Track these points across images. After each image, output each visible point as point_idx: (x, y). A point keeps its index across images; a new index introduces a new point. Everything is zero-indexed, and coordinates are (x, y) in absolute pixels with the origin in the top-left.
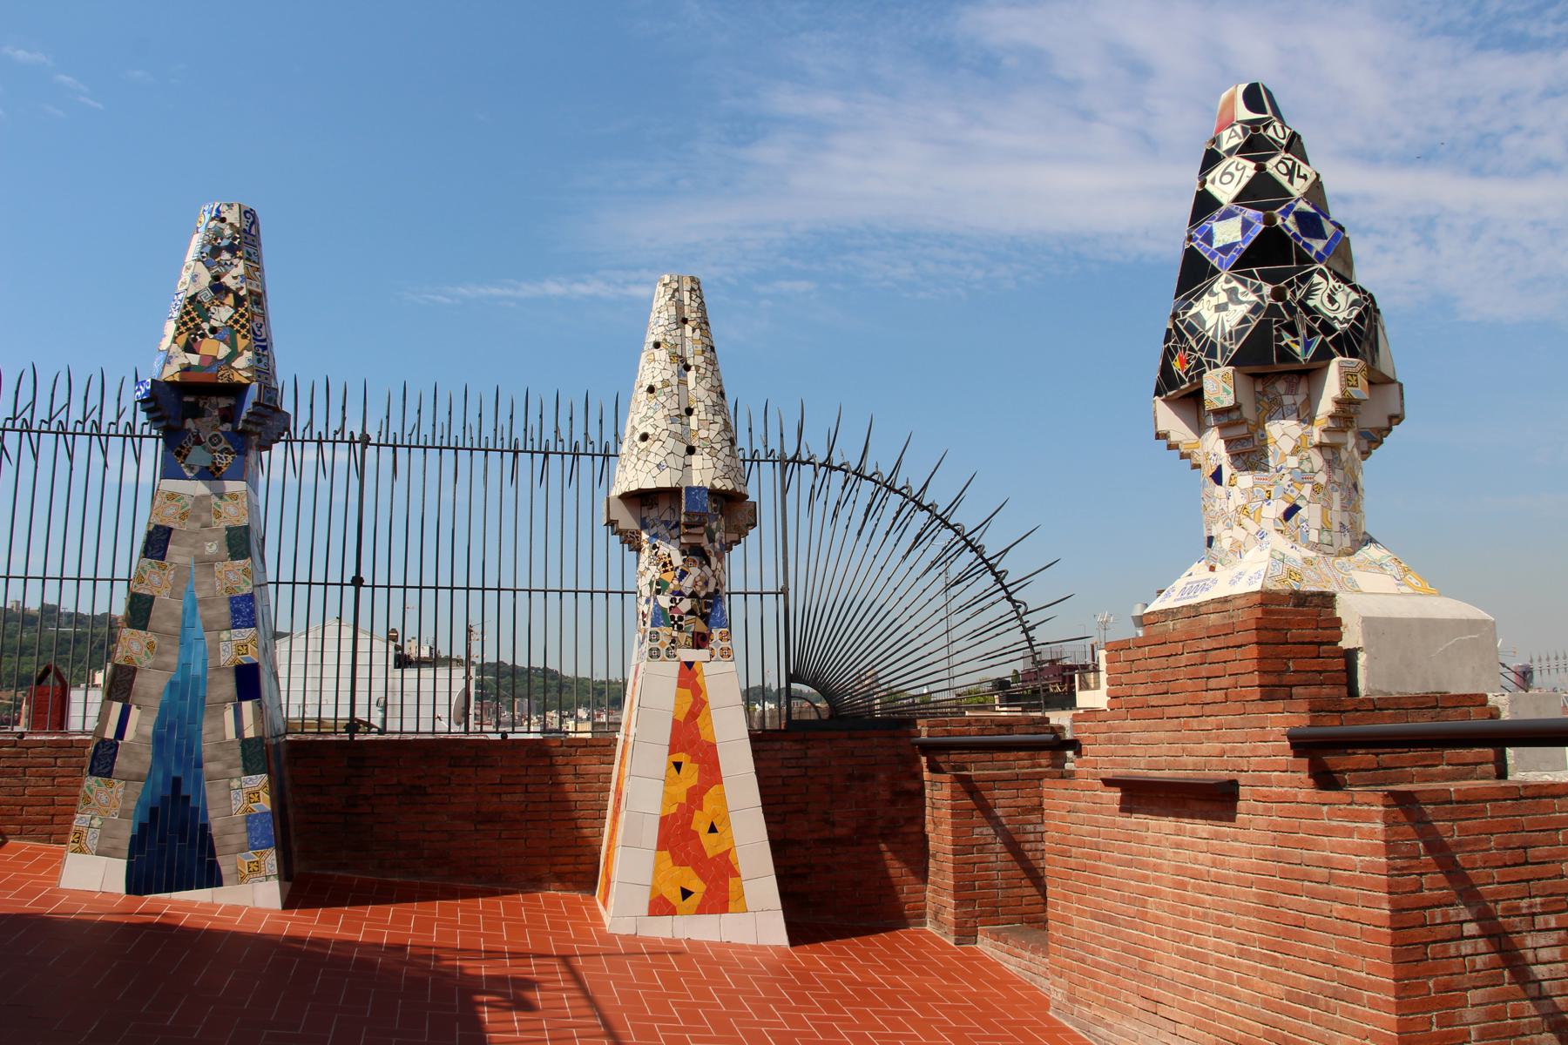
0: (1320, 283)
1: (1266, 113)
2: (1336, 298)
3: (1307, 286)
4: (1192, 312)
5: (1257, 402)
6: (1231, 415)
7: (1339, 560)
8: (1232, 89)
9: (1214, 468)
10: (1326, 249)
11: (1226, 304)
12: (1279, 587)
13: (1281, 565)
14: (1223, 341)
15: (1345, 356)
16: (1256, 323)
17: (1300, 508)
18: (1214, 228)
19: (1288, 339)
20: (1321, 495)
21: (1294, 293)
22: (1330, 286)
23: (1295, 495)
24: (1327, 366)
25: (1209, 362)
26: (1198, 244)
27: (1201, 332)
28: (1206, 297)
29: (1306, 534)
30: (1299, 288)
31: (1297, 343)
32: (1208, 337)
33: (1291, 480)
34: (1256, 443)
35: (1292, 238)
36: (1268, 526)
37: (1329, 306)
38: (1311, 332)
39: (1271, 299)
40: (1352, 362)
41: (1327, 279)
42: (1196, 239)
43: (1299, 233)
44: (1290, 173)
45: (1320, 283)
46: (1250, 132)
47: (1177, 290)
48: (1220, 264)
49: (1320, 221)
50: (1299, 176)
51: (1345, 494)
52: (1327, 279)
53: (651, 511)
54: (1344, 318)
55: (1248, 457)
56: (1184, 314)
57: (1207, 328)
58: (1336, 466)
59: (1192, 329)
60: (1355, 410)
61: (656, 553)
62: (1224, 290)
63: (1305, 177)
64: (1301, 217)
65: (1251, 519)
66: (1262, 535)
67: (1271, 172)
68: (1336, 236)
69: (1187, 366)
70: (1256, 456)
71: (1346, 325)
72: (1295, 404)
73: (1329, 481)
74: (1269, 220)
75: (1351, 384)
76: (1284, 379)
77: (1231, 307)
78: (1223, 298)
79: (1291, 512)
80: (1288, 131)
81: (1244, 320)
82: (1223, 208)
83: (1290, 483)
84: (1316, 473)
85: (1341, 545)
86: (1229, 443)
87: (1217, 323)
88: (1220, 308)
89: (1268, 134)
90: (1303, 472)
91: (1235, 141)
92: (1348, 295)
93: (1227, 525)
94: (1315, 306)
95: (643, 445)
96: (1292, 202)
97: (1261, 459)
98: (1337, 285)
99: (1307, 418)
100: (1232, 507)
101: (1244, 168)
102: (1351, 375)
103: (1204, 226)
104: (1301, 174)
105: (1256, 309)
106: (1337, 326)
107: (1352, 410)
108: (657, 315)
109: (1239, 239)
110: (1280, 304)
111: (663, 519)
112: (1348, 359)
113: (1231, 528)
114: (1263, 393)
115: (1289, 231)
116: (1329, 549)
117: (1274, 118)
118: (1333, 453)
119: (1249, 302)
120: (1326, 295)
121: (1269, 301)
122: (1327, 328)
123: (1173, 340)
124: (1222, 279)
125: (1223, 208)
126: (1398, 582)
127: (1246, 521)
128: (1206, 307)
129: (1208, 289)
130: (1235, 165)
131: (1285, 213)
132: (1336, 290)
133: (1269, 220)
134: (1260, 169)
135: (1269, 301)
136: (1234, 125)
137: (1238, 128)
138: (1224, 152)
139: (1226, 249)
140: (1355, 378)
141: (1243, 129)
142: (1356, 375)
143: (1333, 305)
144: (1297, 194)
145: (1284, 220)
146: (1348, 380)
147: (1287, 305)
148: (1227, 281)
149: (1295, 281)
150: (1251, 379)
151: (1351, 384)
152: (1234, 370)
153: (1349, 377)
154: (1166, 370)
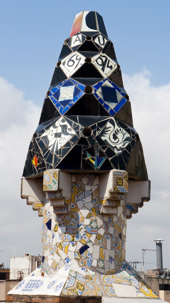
0: (110, 127)
1: (96, 29)
2: (118, 136)
4: (44, 135)
5: (72, 187)
6: (56, 195)
7: (107, 277)
8: (81, 13)
9: (48, 220)
10: (116, 108)
11: (60, 134)
12: (71, 294)
13: (74, 281)
14: (56, 154)
15: (117, 169)
16: (73, 147)
17: (89, 247)
18: (61, 90)
19: (89, 157)
20: (100, 241)
21: (95, 132)
22: (115, 129)
24: (108, 173)
25: (48, 165)
26: (52, 98)
27: (46, 147)
28: (51, 128)
29: (90, 262)
30: (98, 130)
31: (94, 160)
32: (49, 151)
33: (85, 232)
34: (69, 210)
36: (71, 256)
37: (113, 140)
38: (102, 154)
39: (83, 135)
40: (121, 173)
41: (114, 125)
42: (51, 94)
43: (103, 99)
44: (103, 65)
45: (110, 127)
46: (86, 39)
47: (40, 121)
48: (61, 111)
49: (115, 93)
50: (108, 66)
51: (113, 240)
52: (114, 125)
54: (120, 147)
55: (65, 217)
56: (40, 135)
57: (49, 146)
58: (110, 225)
59: (41, 144)
60: (121, 198)
63: (111, 67)
64: (105, 90)
65: (63, 251)
66: (68, 260)
67: (93, 63)
68: (123, 101)
69: (38, 164)
70: (69, 217)
71: (120, 151)
73: (105, 233)
74: (88, 90)
75: (119, 184)
76: (87, 176)
77: (63, 136)
78: (59, 130)
79: (84, 249)
80: (106, 41)
81: (68, 144)
82: (67, 80)
83: (84, 233)
84: (99, 229)
85: (109, 268)
86: (56, 208)
87: (55, 143)
88: (57, 135)
89: (95, 41)
90: (92, 227)
91: (78, 43)
92: (124, 135)
93: (51, 252)
94: (105, 140)
96: (102, 81)
98: (119, 129)
99: (97, 199)
100: (54, 243)
101: (80, 59)
102: (120, 179)
103: (56, 88)
104: (109, 65)
105: (74, 139)
106: (116, 151)
107: (119, 197)
109: (72, 98)
110: (87, 137)
112: (119, 170)
113: (53, 254)
114: (75, 183)
115: (98, 97)
116: (102, 271)
117: (100, 33)
118: (109, 218)
119: (71, 135)
120: (112, 134)
121: (81, 135)
122: (110, 152)
123: (33, 149)
124: (61, 119)
125: (67, 80)
126: (137, 290)
127: (61, 252)
128: (51, 133)
129: (53, 124)
130: (75, 56)
131: (97, 87)
132: (118, 131)
133: (88, 90)
134: (88, 60)
135: (81, 135)
136: (78, 34)
137: (80, 36)
138: (72, 48)
139: (65, 102)
140: (121, 181)
141: (83, 37)
143: (115, 140)
144: (105, 77)
145: (95, 91)
146: (118, 182)
147: (91, 139)
148: (63, 121)
149: (97, 125)
150: (70, 175)
151: (119, 184)
152: (59, 171)
153: (118, 181)
154: (28, 163)
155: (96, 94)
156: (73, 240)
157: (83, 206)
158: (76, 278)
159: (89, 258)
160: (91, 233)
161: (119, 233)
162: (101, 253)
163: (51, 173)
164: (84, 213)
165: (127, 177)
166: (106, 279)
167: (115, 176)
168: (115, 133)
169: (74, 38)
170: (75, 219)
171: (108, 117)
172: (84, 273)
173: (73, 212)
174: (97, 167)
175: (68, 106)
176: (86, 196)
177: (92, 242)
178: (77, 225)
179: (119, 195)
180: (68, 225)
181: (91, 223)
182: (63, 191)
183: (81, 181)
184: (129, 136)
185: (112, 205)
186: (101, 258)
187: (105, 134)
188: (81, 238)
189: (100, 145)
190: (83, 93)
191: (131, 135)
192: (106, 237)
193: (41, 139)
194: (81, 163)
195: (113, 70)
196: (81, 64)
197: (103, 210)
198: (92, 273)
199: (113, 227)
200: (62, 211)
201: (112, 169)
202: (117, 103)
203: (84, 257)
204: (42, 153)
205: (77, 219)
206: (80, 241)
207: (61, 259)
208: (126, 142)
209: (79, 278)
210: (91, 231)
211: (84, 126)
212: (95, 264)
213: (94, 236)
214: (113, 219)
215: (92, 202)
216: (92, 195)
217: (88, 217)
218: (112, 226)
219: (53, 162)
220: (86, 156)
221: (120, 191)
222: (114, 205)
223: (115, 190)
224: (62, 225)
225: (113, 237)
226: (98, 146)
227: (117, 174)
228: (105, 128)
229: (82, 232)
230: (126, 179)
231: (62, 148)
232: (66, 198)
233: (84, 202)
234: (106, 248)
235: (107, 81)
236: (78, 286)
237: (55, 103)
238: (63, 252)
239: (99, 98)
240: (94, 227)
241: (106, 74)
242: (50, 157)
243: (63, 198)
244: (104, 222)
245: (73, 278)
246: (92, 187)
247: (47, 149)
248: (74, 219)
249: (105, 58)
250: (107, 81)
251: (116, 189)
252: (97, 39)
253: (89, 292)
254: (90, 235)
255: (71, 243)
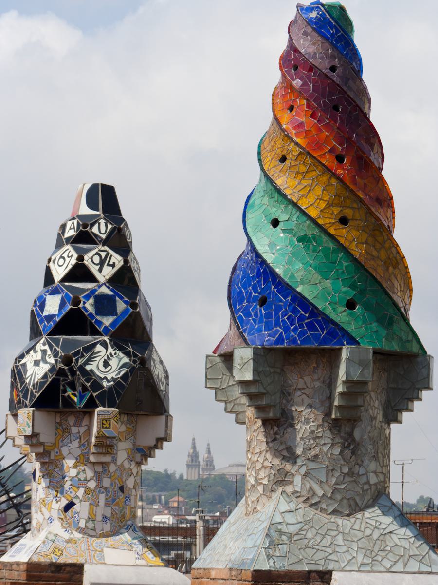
1: (98, 210)
2: (110, 362)
3: (89, 354)
5: (57, 429)
6: (32, 440)
7: (98, 540)
9: (34, 469)
10: (113, 324)
12: (42, 560)
13: (50, 545)
14: (32, 388)
15: (104, 406)
16: (51, 380)
17: (75, 504)
19: (69, 392)
20: (90, 496)
21: (77, 360)
22: (108, 353)
23: (72, 495)
29: (77, 522)
30: (83, 356)
31: (75, 395)
33: (71, 485)
35: (88, 317)
36: (55, 515)
37: (102, 368)
38: (85, 389)
40: (108, 411)
41: (107, 348)
44: (102, 263)
49: (115, 301)
50: (109, 265)
51: (110, 495)
52: (107, 348)
54: (112, 378)
57: (27, 377)
59: (19, 373)
62: (41, 350)
63: (113, 265)
66: (51, 520)
72: (79, 433)
73: (97, 487)
75: (104, 426)
77: (42, 364)
78: (39, 356)
79: (69, 506)
81: (45, 376)
82: (54, 285)
83: (70, 487)
84: (88, 481)
85: (102, 530)
87: (32, 374)
89: (93, 230)
90: (80, 480)
92: (120, 360)
94: (91, 370)
97: (55, 469)
98: (113, 353)
99: (86, 443)
101: (72, 256)
102: (106, 420)
104: (111, 263)
106: (105, 384)
109: (57, 313)
112: (106, 409)
114: (60, 424)
115: (87, 310)
116: (91, 533)
122: (97, 385)
125: (54, 285)
126: (139, 557)
127: (44, 509)
131: (88, 297)
132: (112, 356)
134: (80, 258)
136: (74, 219)
139: (50, 318)
140: (108, 422)
142: (109, 420)
143: (106, 368)
145: (84, 303)
146: (103, 424)
147: (71, 370)
148: (44, 344)
149: (81, 350)
152: (33, 411)
153: (104, 422)
155: (84, 308)
156: (57, 495)
157: (68, 452)
158: (55, 542)
159: (76, 517)
160: (77, 486)
161: (119, 485)
162: (91, 511)
163: (25, 413)
164: (69, 462)
165: (116, 416)
166: (97, 543)
167: (99, 417)
168: (106, 359)
169: (69, 224)
170: (60, 470)
171: (99, 338)
172: (66, 536)
173: (57, 460)
174: (80, 405)
175: (52, 323)
176: (72, 440)
177: (79, 498)
178: (61, 477)
179: (108, 439)
180: (52, 476)
181: (78, 474)
182: (41, 435)
183: (66, 420)
184: (129, 361)
185: (101, 451)
186: (90, 517)
187: (92, 361)
188: (66, 493)
189: (83, 377)
190: (69, 307)
191: (130, 360)
192: (97, 491)
193: (20, 367)
194: (61, 401)
195: (116, 269)
196: (71, 264)
197: (92, 458)
198: (77, 535)
199: (109, 478)
200: (43, 459)
201: (98, 407)
202: (117, 316)
203: (69, 516)
204: (19, 386)
205: (62, 468)
206: (65, 497)
207: (44, 519)
208: (122, 370)
209: (58, 541)
210: (78, 483)
211: (64, 353)
212: (82, 524)
213: (82, 490)
214: (108, 468)
215: (79, 447)
216: (80, 439)
217: (74, 467)
218: (108, 477)
219: (28, 399)
220: (65, 391)
221: (107, 435)
222: (104, 451)
223: (99, 434)
224: (46, 477)
225: (109, 491)
226: (80, 378)
227: (102, 413)
228: (94, 353)
229: (67, 486)
230: (115, 419)
231: (39, 381)
232: (47, 443)
233: (70, 448)
234: (98, 505)
235: (104, 286)
236: (55, 551)
237: (38, 318)
238: (46, 510)
239: (88, 313)
240: (82, 479)
241: (104, 276)
242: (26, 391)
243: (42, 444)
244: (95, 472)
245: (49, 541)
246: (80, 428)
247: (25, 381)
248: (58, 469)
249: (106, 253)
250: (104, 286)
251: (101, 433)
252: (96, 226)
253: (68, 557)
254: (77, 488)
255: (55, 499)
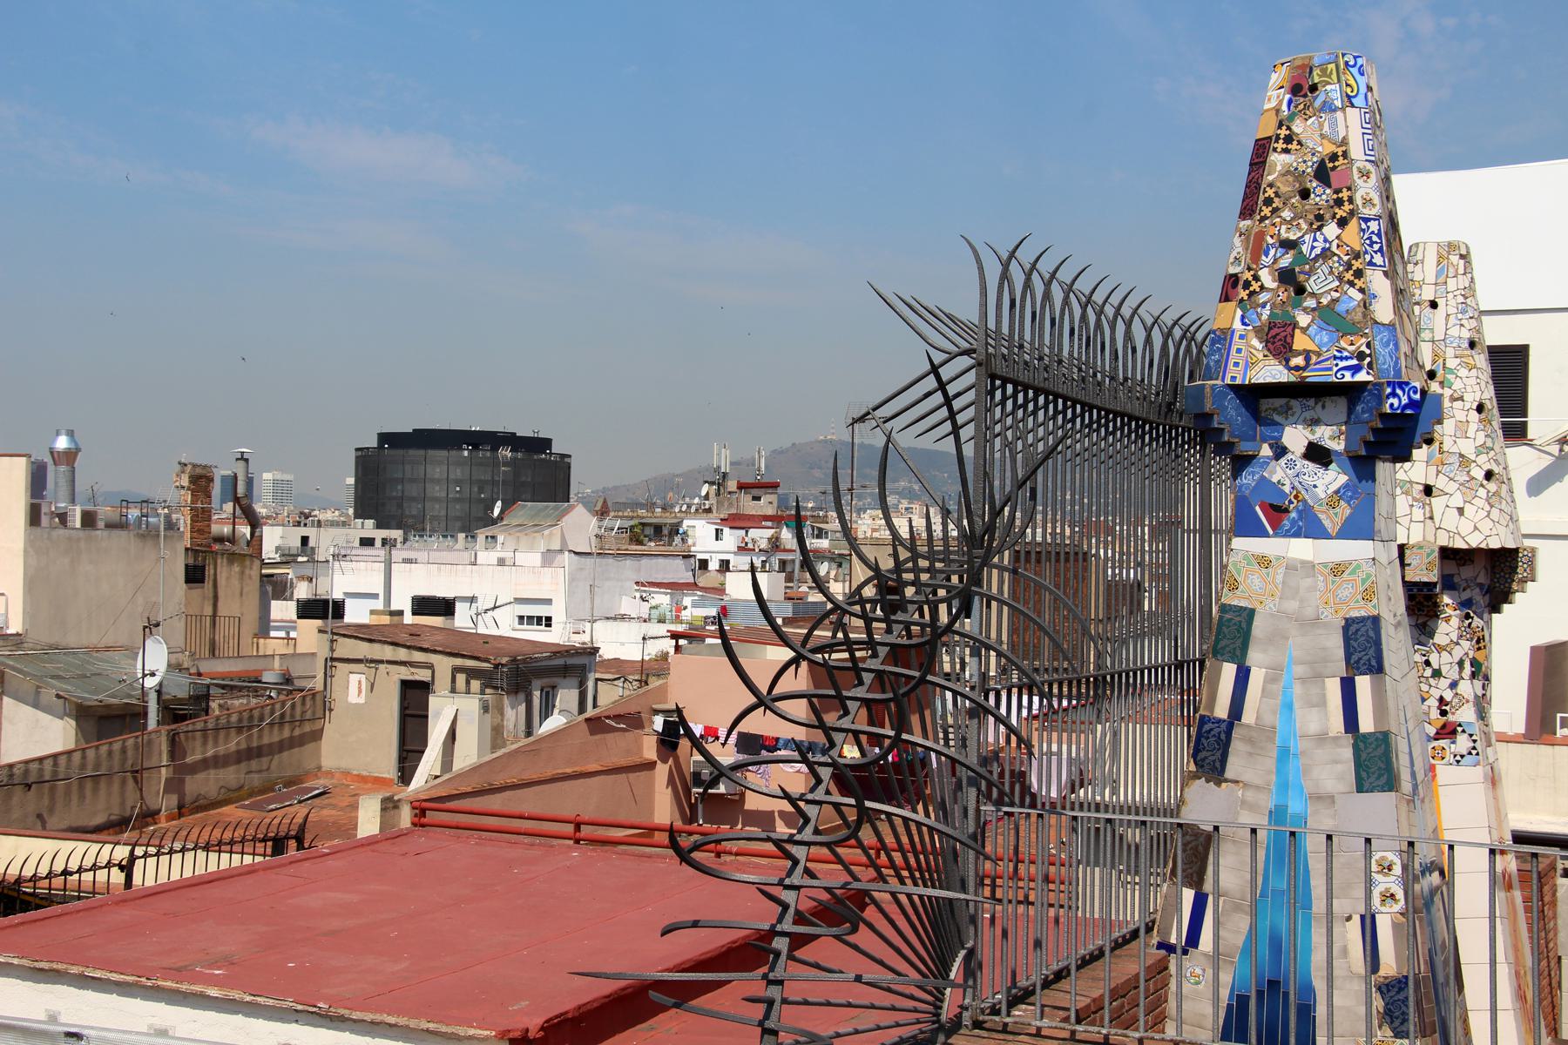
53: (1461, 568)
61: (1470, 624)
95: (1492, 486)
108: (1461, 299)
111: (1478, 581)
